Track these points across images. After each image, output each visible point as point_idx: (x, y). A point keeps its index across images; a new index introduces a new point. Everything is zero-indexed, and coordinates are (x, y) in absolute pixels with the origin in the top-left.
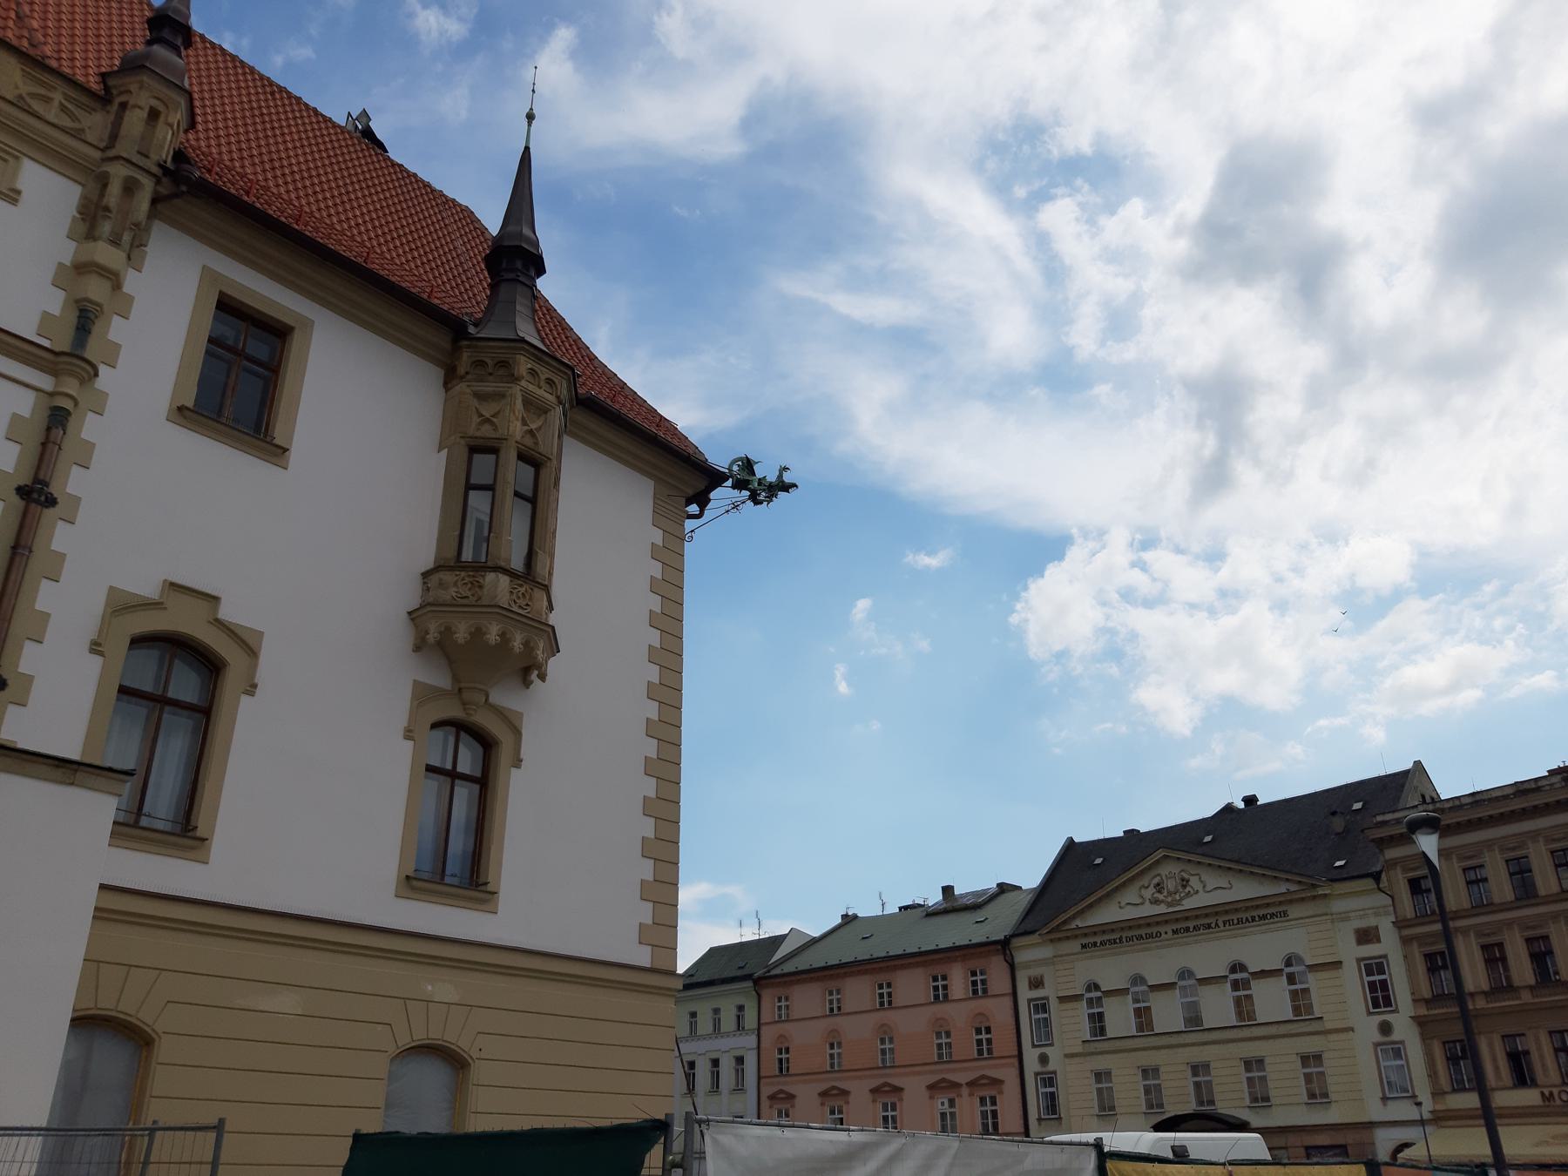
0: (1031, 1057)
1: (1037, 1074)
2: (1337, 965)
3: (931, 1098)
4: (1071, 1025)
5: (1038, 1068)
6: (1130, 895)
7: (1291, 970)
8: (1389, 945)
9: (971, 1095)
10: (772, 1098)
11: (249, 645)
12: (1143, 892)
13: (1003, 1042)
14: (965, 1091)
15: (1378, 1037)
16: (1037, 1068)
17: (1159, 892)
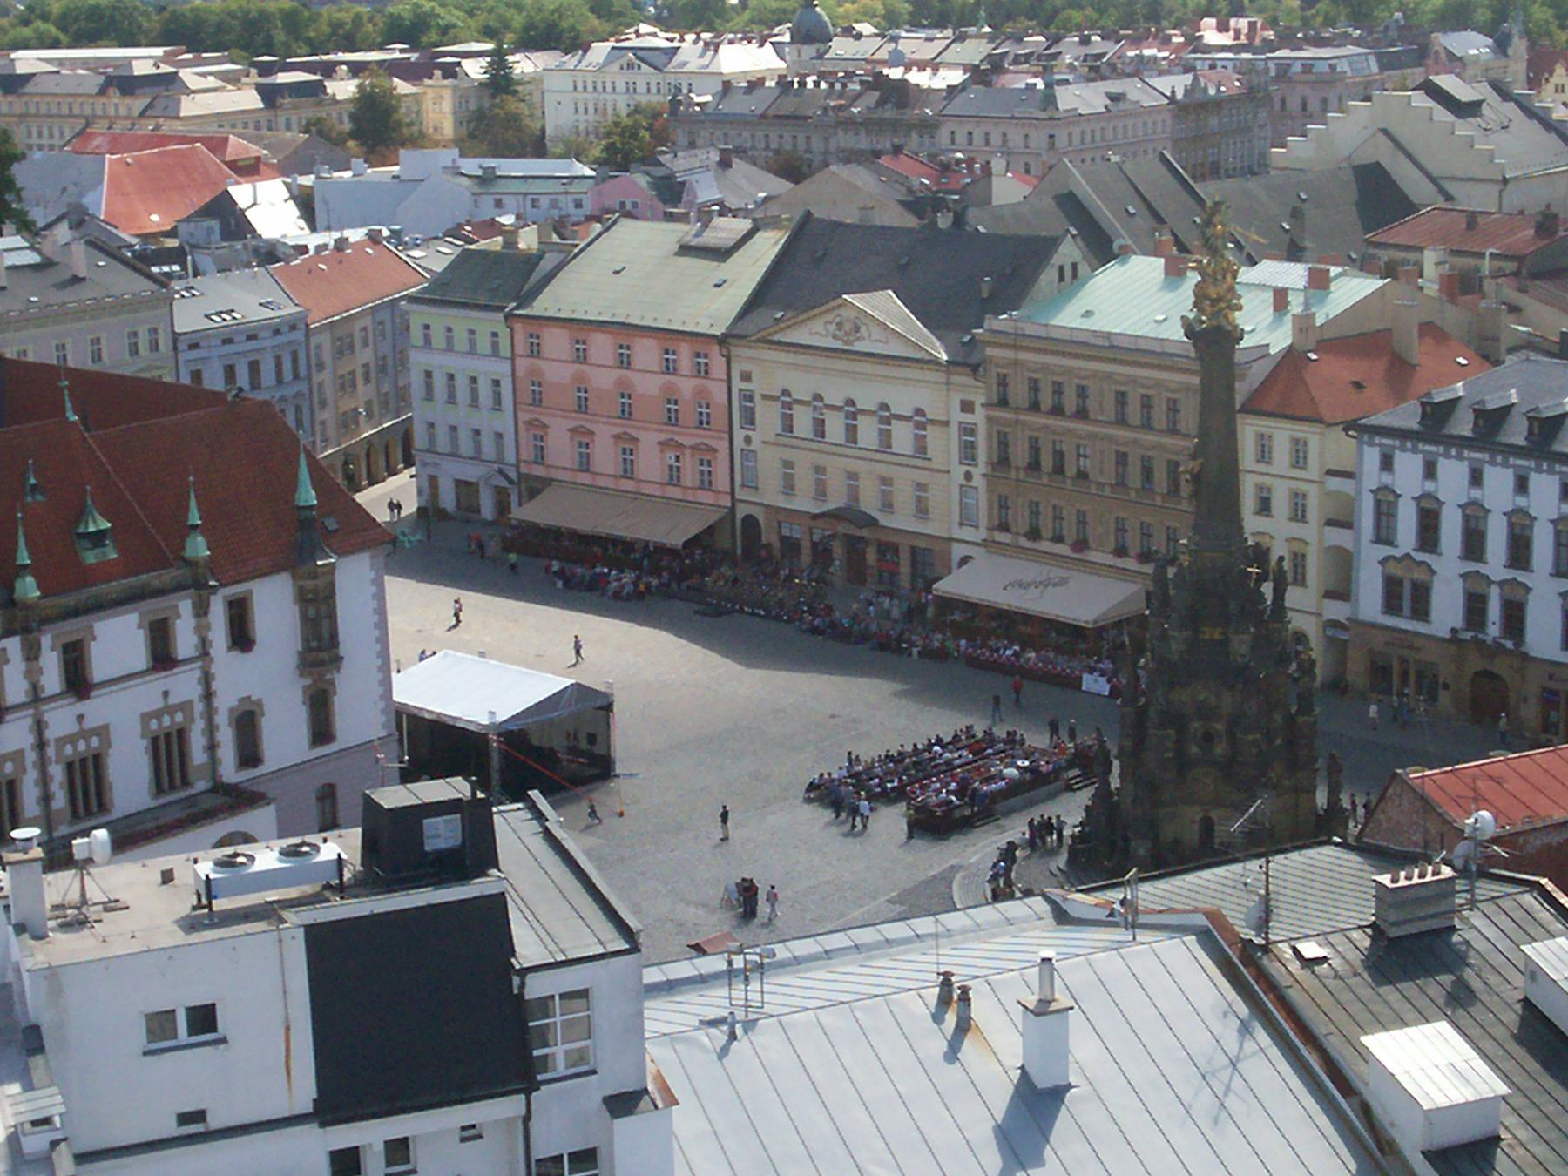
0: (739, 435)
1: (742, 450)
2: (946, 423)
3: (662, 451)
4: (768, 417)
5: (743, 446)
6: (818, 325)
7: (920, 420)
8: (978, 417)
9: (693, 456)
10: (529, 423)
11: (259, 703)
12: (829, 326)
13: (719, 421)
14: (688, 452)
15: (964, 482)
16: (743, 446)
17: (839, 329)
